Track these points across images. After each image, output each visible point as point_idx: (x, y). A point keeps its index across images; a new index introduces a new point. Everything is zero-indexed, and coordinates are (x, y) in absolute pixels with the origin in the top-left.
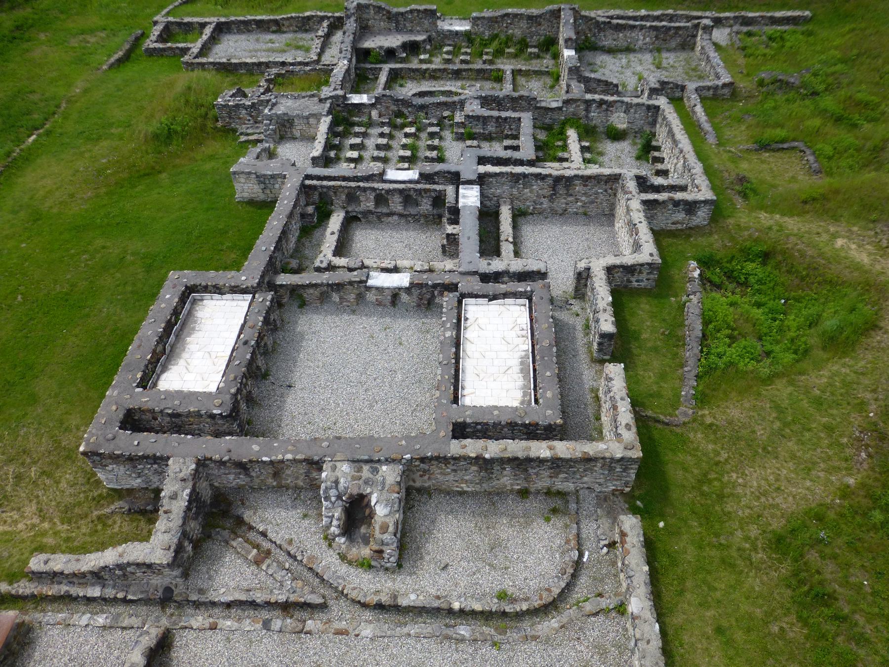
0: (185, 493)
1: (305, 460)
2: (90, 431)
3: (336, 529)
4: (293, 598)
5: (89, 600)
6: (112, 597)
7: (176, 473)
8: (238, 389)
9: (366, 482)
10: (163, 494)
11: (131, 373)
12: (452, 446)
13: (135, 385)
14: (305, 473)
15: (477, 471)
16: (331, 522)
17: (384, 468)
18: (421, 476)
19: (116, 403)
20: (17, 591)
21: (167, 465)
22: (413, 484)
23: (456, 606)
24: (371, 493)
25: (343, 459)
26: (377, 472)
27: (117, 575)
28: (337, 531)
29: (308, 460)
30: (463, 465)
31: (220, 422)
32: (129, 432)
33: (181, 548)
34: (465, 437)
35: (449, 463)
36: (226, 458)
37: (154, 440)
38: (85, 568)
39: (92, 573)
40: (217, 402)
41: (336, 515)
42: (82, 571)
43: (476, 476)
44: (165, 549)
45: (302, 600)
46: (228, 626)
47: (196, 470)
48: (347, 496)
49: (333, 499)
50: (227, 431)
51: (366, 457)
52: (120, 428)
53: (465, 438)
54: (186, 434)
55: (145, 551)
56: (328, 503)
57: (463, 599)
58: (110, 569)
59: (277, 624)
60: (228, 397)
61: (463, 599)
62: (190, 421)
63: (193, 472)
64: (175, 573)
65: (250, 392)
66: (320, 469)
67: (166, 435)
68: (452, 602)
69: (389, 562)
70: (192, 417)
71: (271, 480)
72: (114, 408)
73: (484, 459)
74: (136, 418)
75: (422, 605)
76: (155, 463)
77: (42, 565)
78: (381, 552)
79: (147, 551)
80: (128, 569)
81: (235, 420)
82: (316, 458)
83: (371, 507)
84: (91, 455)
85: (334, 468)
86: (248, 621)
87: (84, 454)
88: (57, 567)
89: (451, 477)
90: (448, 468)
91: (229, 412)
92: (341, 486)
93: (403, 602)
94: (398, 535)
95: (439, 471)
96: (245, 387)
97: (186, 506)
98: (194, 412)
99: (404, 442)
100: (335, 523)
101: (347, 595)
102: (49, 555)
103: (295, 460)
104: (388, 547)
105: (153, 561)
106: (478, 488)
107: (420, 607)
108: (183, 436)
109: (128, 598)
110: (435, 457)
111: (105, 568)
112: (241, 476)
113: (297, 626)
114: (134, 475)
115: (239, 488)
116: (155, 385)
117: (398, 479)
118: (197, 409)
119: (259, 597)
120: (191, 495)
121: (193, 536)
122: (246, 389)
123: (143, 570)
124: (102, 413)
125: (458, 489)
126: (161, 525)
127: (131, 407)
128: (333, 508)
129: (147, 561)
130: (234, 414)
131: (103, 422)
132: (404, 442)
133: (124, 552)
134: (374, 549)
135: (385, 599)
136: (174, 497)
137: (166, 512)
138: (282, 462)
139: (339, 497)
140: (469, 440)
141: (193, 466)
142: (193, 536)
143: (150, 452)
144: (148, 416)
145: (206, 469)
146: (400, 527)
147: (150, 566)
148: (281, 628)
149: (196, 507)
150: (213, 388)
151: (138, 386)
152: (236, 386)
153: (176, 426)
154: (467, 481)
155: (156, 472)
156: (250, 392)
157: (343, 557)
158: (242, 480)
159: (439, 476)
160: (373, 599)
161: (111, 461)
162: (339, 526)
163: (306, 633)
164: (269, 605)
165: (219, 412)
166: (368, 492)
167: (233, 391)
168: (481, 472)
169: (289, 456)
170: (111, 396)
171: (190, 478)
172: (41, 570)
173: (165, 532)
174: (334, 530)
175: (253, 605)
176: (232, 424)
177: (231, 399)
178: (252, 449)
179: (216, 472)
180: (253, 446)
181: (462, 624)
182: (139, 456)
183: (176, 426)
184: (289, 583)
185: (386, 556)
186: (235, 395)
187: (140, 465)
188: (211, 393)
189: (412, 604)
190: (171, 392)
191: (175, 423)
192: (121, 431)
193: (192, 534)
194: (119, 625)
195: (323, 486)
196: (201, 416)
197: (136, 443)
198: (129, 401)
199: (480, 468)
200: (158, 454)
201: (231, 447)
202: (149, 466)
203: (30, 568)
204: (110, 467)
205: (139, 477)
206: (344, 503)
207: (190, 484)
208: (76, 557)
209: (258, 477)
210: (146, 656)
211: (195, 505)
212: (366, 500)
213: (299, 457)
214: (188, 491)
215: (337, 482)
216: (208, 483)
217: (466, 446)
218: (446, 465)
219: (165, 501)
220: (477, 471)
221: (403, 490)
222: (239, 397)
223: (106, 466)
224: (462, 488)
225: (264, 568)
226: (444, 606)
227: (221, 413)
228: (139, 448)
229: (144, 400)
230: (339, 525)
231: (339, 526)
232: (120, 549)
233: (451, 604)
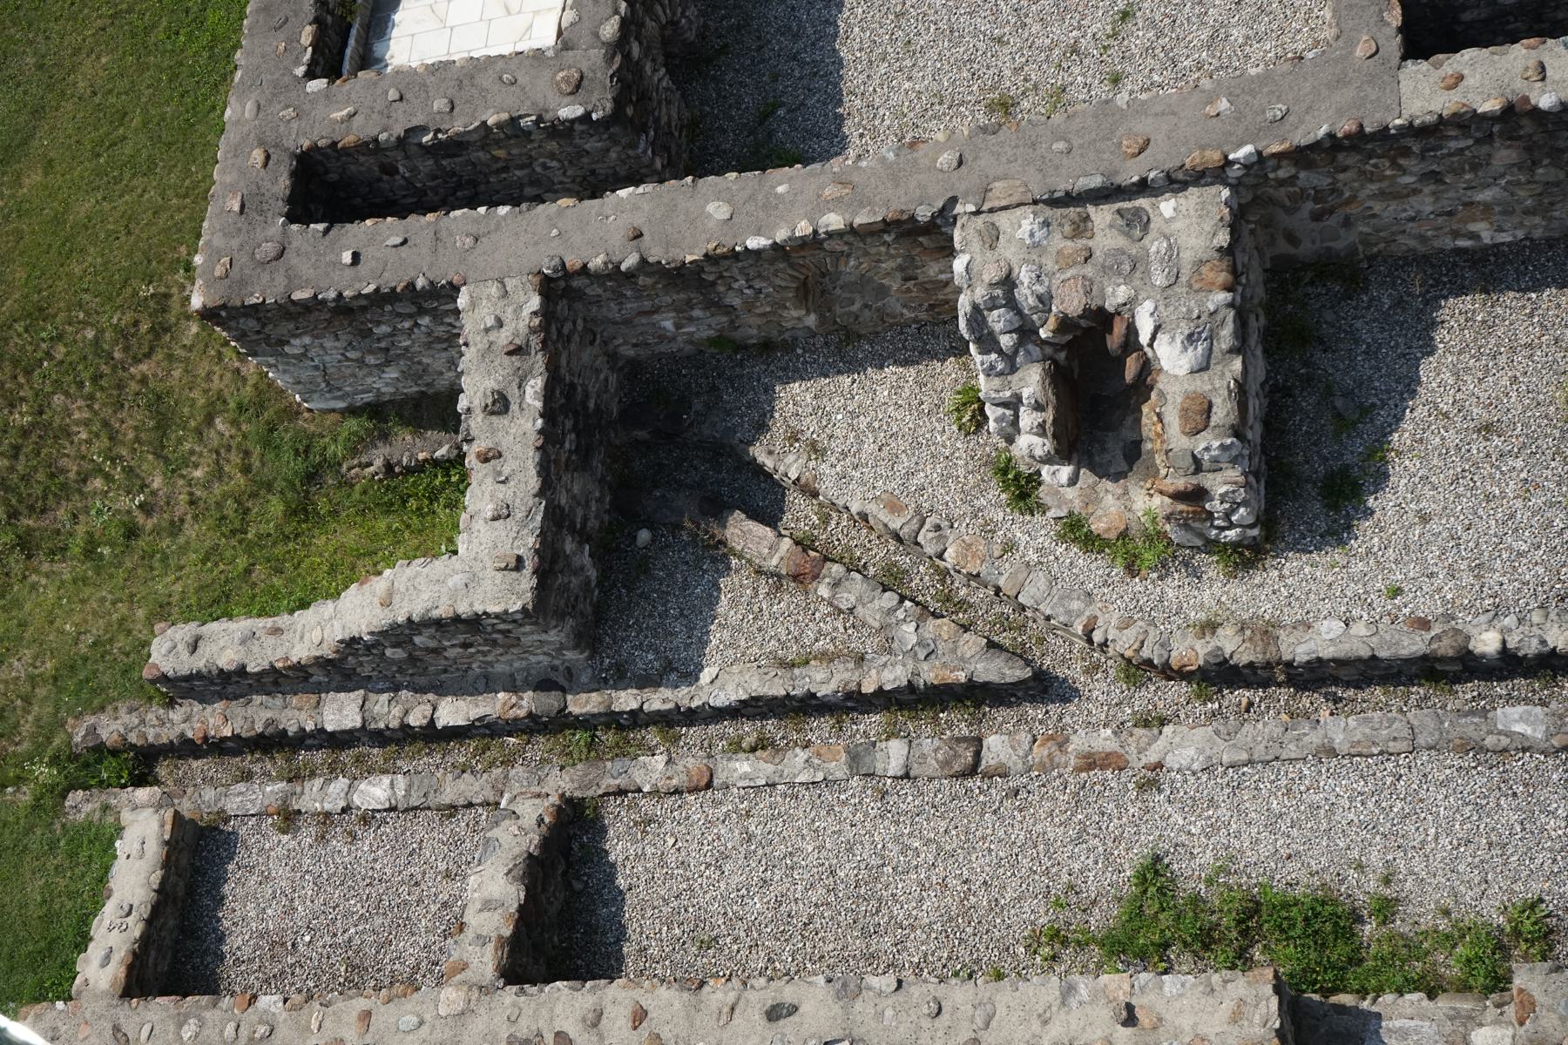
0: (529, 391)
1: (887, 225)
2: (208, 243)
3: (1037, 440)
4: (930, 674)
5: (339, 741)
6: (394, 724)
7: (487, 330)
8: (624, 23)
9: (1111, 269)
10: (462, 404)
11: (281, 35)
12: (1406, 86)
13: (300, 71)
14: (901, 268)
15: (1519, 166)
16: (1017, 416)
17: (1167, 206)
18: (1317, 217)
19: (261, 143)
20: (144, 736)
21: (457, 312)
22: (1292, 250)
23: (1487, 643)
24: (1131, 303)
25: (1015, 200)
26: (1146, 227)
27: (393, 662)
28: (1042, 446)
29: (897, 223)
30: (1461, 151)
31: (592, 144)
32: (321, 227)
33: (553, 561)
34: (1454, 45)
35: (1406, 152)
36: (630, 262)
37: (399, 240)
38: (301, 652)
39: (321, 663)
40: (566, 80)
41: (1026, 393)
42: (295, 660)
43: (1518, 183)
44: (505, 569)
45: (962, 677)
46: (744, 777)
47: (547, 314)
48: (1052, 323)
49: (1006, 341)
50: (622, 172)
51: (1096, 181)
52: (292, 218)
53: (1455, 49)
54: (493, 204)
55: (450, 583)
56: (994, 356)
57: (1510, 621)
58: (369, 647)
59: (894, 754)
60: (597, 55)
61: (1510, 621)
62: (496, 159)
63: (537, 321)
64: (553, 636)
65: (673, 23)
66: (949, 251)
67: (430, 217)
68: (1469, 629)
69: (1231, 526)
70: (498, 143)
71: (795, 313)
72: (258, 156)
73: (1536, 112)
74: (333, 177)
75: (1365, 653)
76: (422, 312)
77: (185, 655)
78: (1197, 495)
79: (457, 580)
80: (417, 640)
81: (644, 129)
82: (924, 214)
83: (1140, 348)
84: (231, 318)
85: (993, 237)
86: (802, 755)
87: (209, 315)
88: (227, 659)
89: (1425, 203)
90: (1404, 172)
91: (609, 106)
92: (1026, 295)
93: (1299, 649)
94: (1255, 434)
95: (1374, 187)
96: (649, 10)
97: (540, 432)
98: (499, 125)
99: (1223, 104)
100: (1027, 419)
101: (1104, 645)
102: (193, 625)
103: (852, 230)
104: (1219, 477)
105: (479, 608)
106: (1538, 227)
107: (1359, 660)
108: (482, 210)
109: (440, 724)
110: (1348, 136)
111: (351, 644)
112: (697, 313)
113: (956, 756)
114: (371, 360)
115: (697, 357)
116: (368, 60)
117: (1223, 238)
118: (505, 116)
119: (823, 681)
120: (548, 394)
121: (585, 519)
122: (656, 19)
123: (461, 638)
124: (228, 179)
125: (1463, 243)
126: (481, 496)
127: (306, 144)
128: (1013, 369)
129: (463, 609)
130: (630, 111)
131: (236, 208)
132: (1223, 104)
133: (390, 593)
134: (1171, 489)
135: (1229, 642)
136: (500, 405)
137: (485, 458)
138: (813, 242)
139: (1026, 332)
140: (1468, 54)
141: (535, 302)
142: (585, 519)
143: (394, 279)
144: (368, 163)
145: (578, 306)
146: (1254, 405)
147: (474, 623)
148: (907, 767)
149: (574, 429)
150: (544, 36)
151: (311, 75)
152: (616, 12)
153: (459, 186)
154: (1487, 208)
155: (432, 341)
156: (673, 23)
157: (1075, 530)
158: (703, 326)
159: (1377, 207)
160: (1191, 650)
161: (291, 326)
162: (1041, 430)
163: (988, 775)
164: (854, 703)
165: (579, 111)
166: (1120, 300)
167: (610, 30)
168: (1535, 163)
169: (834, 221)
170: (238, 122)
171: (535, 341)
172: (185, 671)
173: (494, 519)
174: (1030, 443)
175: (805, 707)
176: (634, 146)
177: (609, 59)
178: (710, 216)
179: (612, 311)
180: (711, 208)
181: (1509, 699)
182: (367, 296)
183: (459, 186)
184: (910, 628)
185: (1216, 506)
186: (620, 45)
187: (379, 323)
188: (539, 53)
189: (1327, 652)
190: (413, 72)
191: (454, 174)
192: (295, 227)
193: (580, 512)
194: (433, 800)
195: (964, 304)
196: (527, 134)
197: (347, 257)
198: (295, 125)
199: (1528, 149)
200: (420, 283)
201: (639, 221)
202: (407, 324)
203: (155, 666)
204: (295, 347)
205: (388, 363)
206: (1049, 350)
207: (539, 361)
208: (269, 622)
209: (749, 306)
210: (522, 878)
211: (569, 424)
212: (1119, 328)
213: (858, 221)
214: (535, 385)
215: (1008, 282)
216: (596, 350)
217: (1461, 78)
218: (1394, 164)
219: (476, 424)
220: (1519, 166)
221: (1256, 276)
222: (636, 50)
223: (283, 342)
224: (1474, 236)
225: (824, 591)
226: (1446, 648)
227: (587, 115)
228: (362, 268)
229: (338, 115)
230: (1042, 426)
231: (1041, 430)
232: (379, 585)
233: (1468, 638)
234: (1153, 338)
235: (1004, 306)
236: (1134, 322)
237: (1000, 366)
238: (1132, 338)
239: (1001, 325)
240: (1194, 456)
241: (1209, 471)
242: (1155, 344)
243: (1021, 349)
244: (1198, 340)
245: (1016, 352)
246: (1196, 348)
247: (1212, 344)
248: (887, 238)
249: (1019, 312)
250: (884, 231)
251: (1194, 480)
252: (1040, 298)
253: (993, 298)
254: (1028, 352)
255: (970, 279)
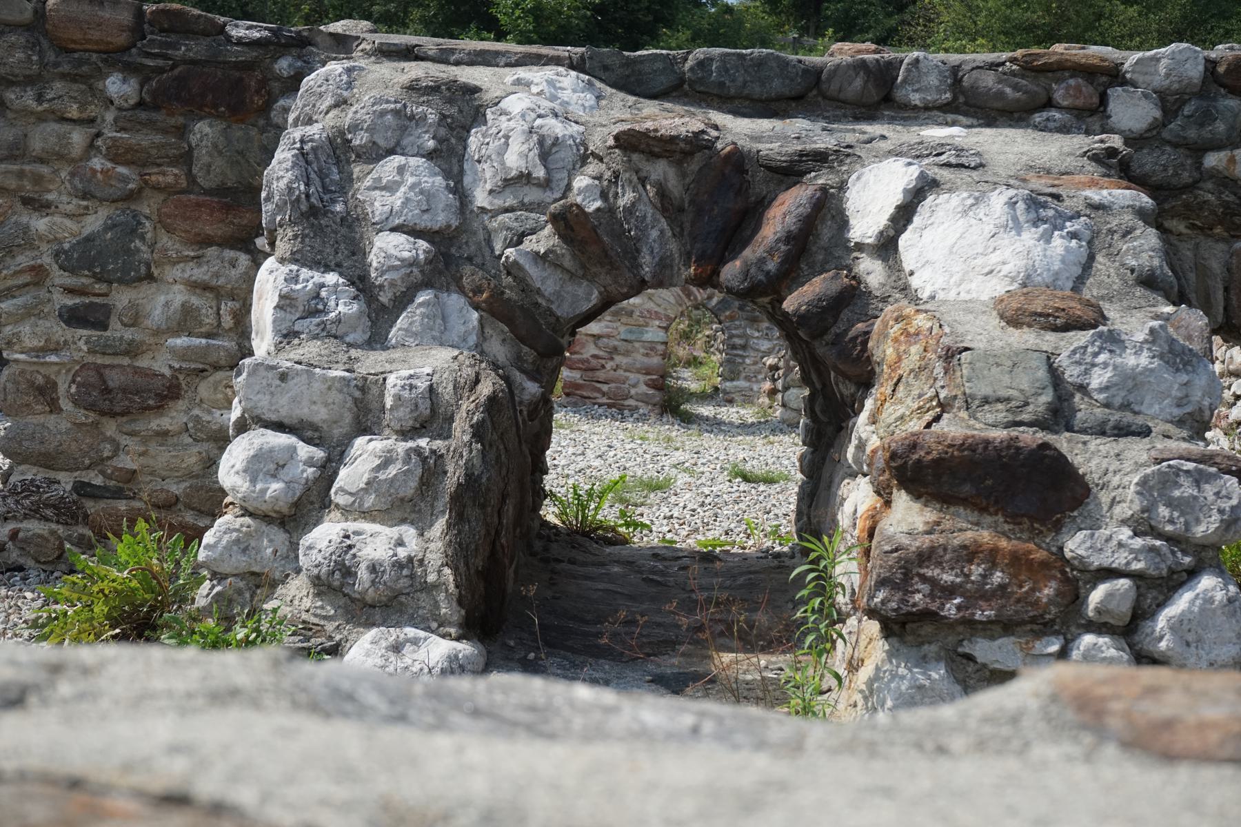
56: (332, 278)
104: (1137, 450)
128: (377, 340)
234: (904, 215)
235: (430, 155)
236: (840, 200)
237: (344, 307)
238: (826, 232)
239: (397, 200)
240: (1055, 376)
241: (1101, 431)
242: (903, 241)
243: (423, 297)
244: (1055, 228)
245: (403, 300)
246: (1047, 238)
247: (1091, 258)
248: (116, 86)
249: (461, 194)
250: (115, 58)
251: (1030, 437)
252: (547, 149)
253: (406, 120)
254: (440, 316)
255: (350, 85)
